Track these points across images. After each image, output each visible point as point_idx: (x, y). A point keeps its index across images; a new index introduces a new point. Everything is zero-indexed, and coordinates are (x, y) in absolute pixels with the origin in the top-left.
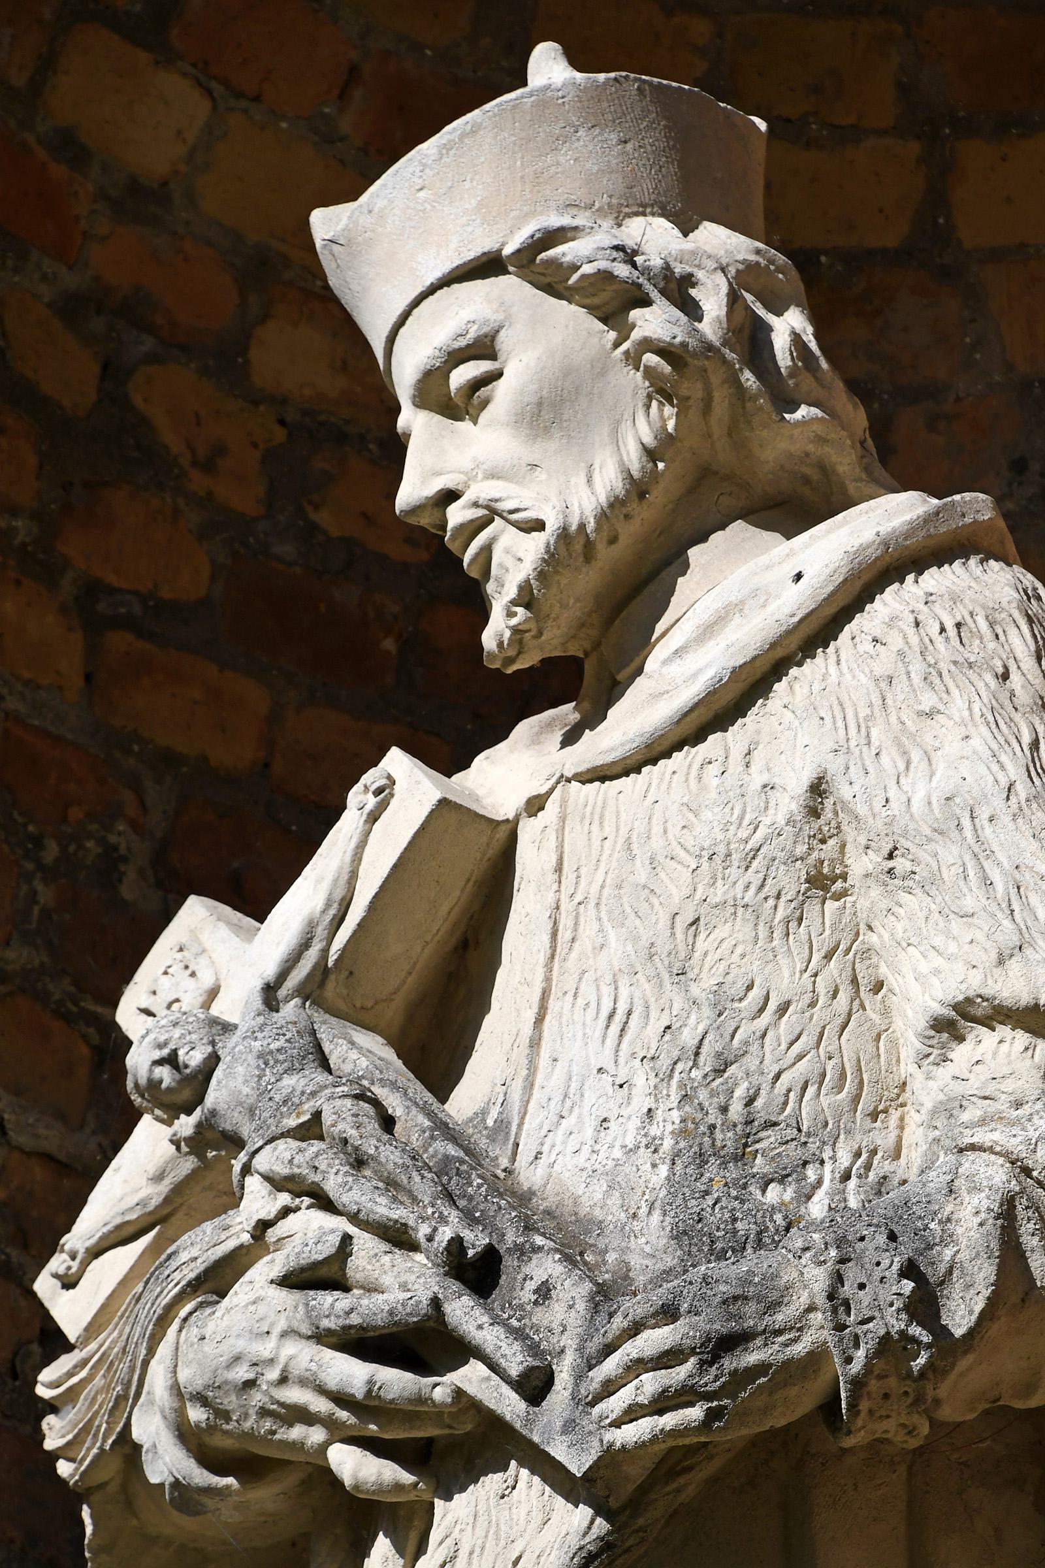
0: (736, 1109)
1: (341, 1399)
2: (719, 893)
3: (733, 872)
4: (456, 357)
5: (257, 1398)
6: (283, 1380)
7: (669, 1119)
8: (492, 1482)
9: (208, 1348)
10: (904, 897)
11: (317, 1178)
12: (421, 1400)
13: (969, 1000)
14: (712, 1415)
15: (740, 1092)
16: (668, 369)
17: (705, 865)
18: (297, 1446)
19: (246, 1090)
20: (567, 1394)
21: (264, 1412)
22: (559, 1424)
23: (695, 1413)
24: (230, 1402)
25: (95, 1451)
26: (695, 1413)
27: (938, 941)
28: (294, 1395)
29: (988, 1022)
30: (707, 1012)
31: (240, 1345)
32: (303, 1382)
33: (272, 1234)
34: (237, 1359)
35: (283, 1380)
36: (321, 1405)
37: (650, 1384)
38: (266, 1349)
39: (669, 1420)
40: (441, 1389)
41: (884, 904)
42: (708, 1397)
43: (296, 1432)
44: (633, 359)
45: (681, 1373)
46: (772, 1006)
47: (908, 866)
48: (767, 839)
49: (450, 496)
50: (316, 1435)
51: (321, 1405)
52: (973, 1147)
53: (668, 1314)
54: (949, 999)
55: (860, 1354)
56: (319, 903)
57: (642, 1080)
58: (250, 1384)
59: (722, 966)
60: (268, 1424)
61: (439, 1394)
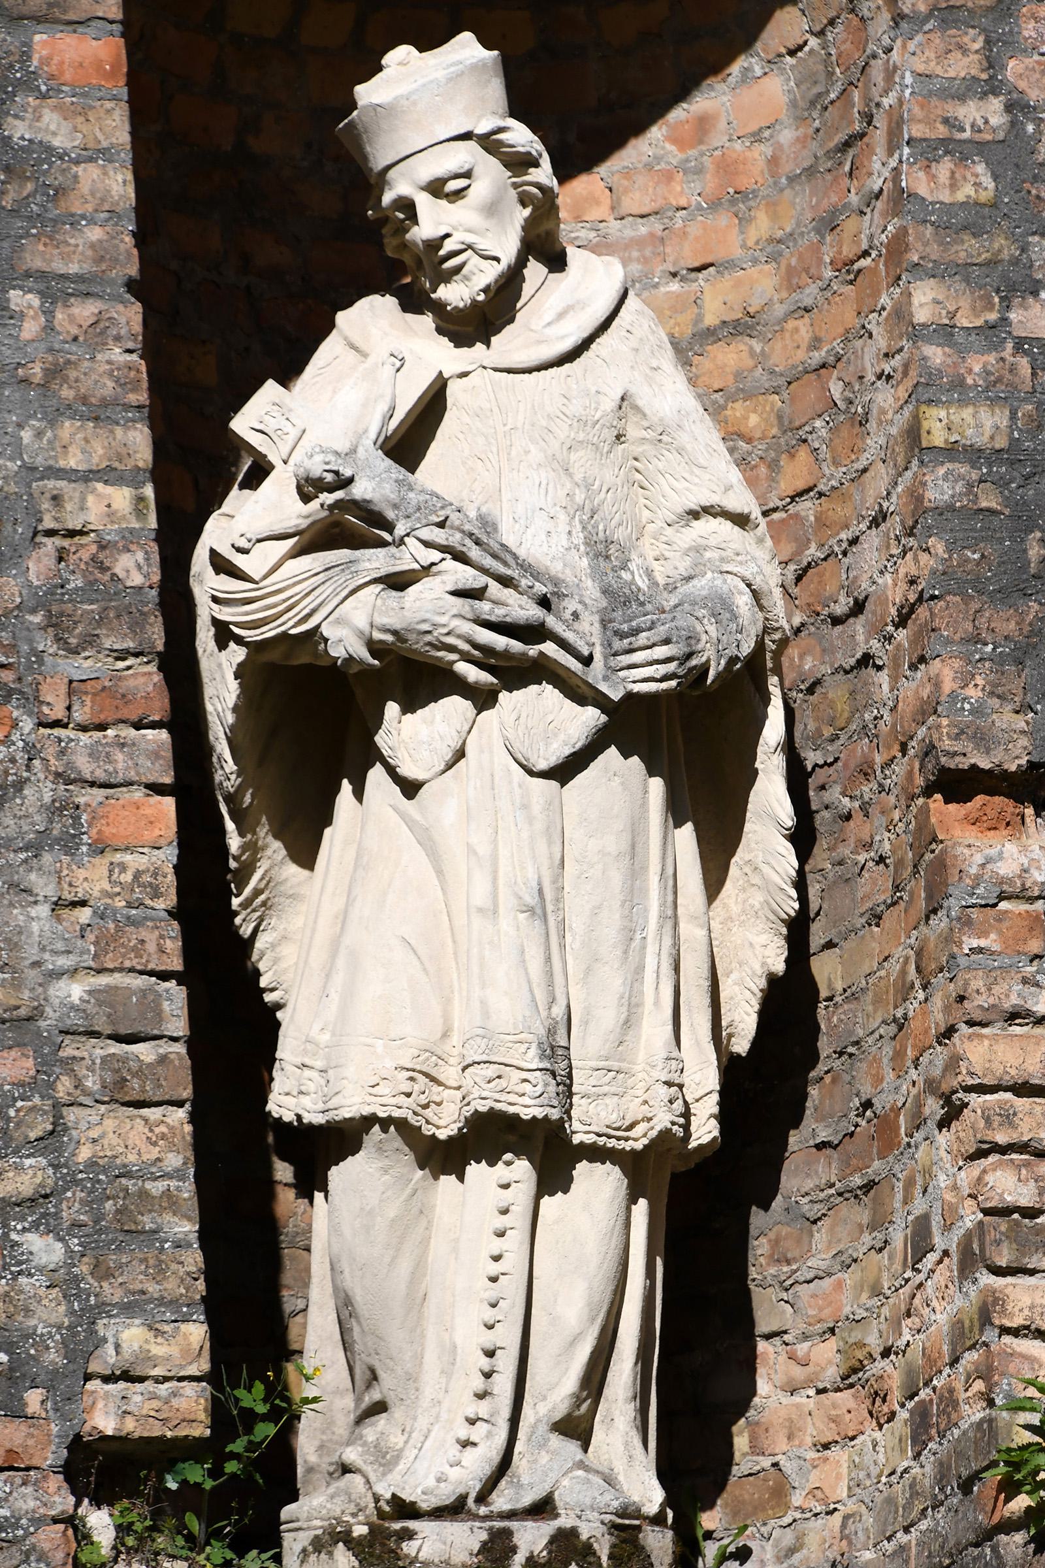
0: (601, 534)
1: (476, 646)
2: (581, 436)
3: (588, 428)
4: (457, 176)
5: (428, 638)
6: (448, 634)
7: (579, 538)
8: (533, 689)
9: (405, 613)
10: (665, 453)
11: (464, 549)
12: (524, 654)
13: (712, 506)
14: (679, 684)
15: (601, 527)
16: (540, 195)
17: (575, 424)
18: (440, 659)
19: (392, 496)
20: (602, 663)
21: (430, 644)
22: (600, 677)
23: (673, 683)
24: (412, 637)
25: (279, 630)
26: (673, 683)
27: (686, 475)
28: (450, 640)
29: (715, 516)
30: (584, 490)
31: (428, 616)
32: (459, 636)
33: (434, 569)
34: (424, 621)
35: (448, 634)
36: (465, 647)
37: (662, 670)
38: (443, 620)
39: (664, 685)
40: (533, 651)
41: (654, 453)
42: (679, 677)
43: (441, 654)
44: (515, 186)
45: (672, 667)
46: (604, 490)
47: (670, 440)
48: (602, 417)
49: (447, 236)
50: (453, 657)
51: (465, 647)
52: (727, 572)
53: (667, 642)
54: (703, 504)
55: (723, 662)
56: (386, 409)
57: (563, 517)
58: (429, 632)
59: (583, 470)
60: (427, 648)
61: (531, 653)
